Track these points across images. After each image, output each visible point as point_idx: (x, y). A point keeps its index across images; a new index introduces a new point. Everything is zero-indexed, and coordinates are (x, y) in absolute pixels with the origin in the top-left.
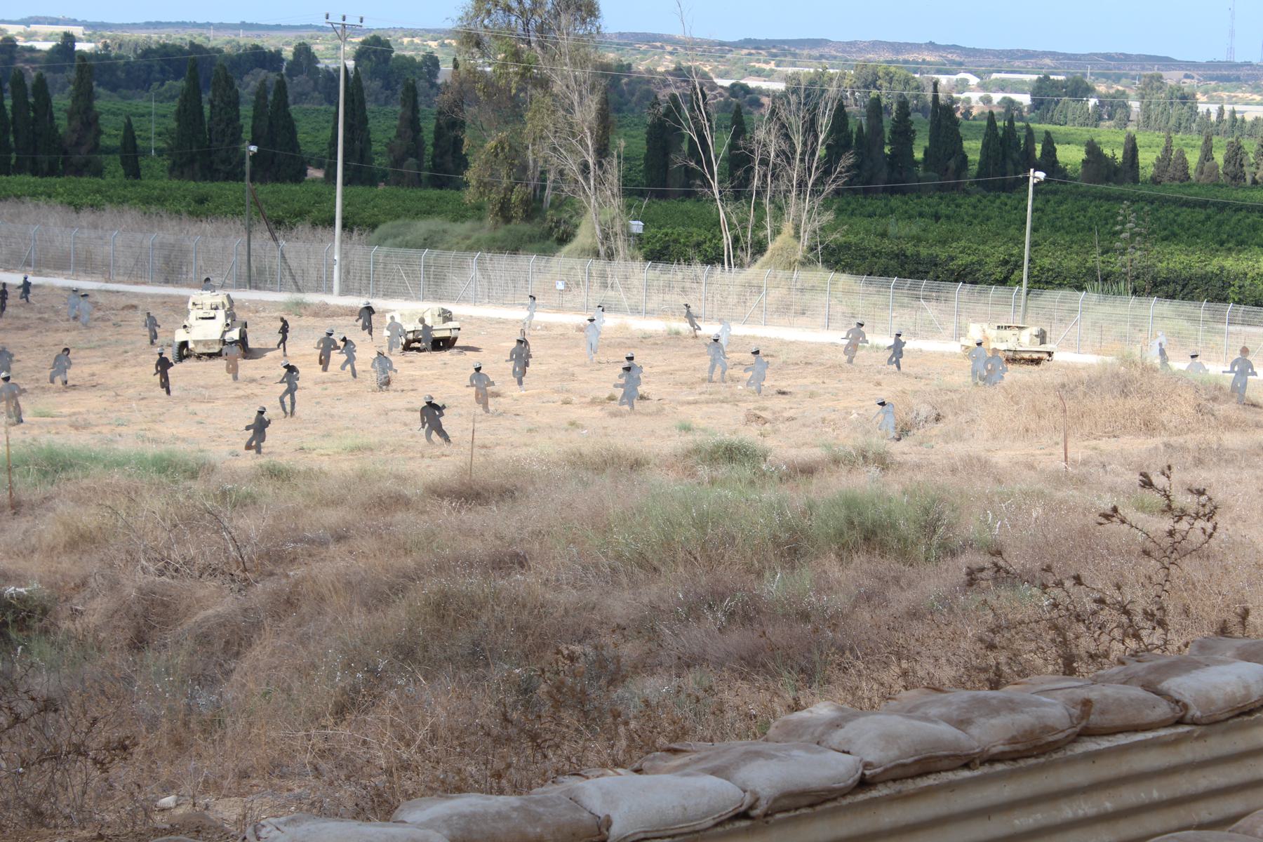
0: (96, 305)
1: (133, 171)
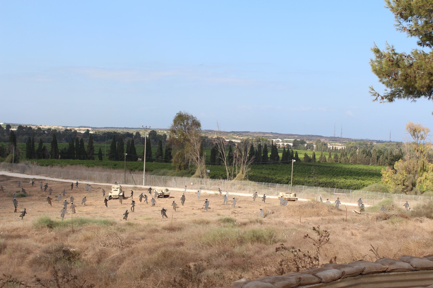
0: (92, 188)
1: (101, 159)
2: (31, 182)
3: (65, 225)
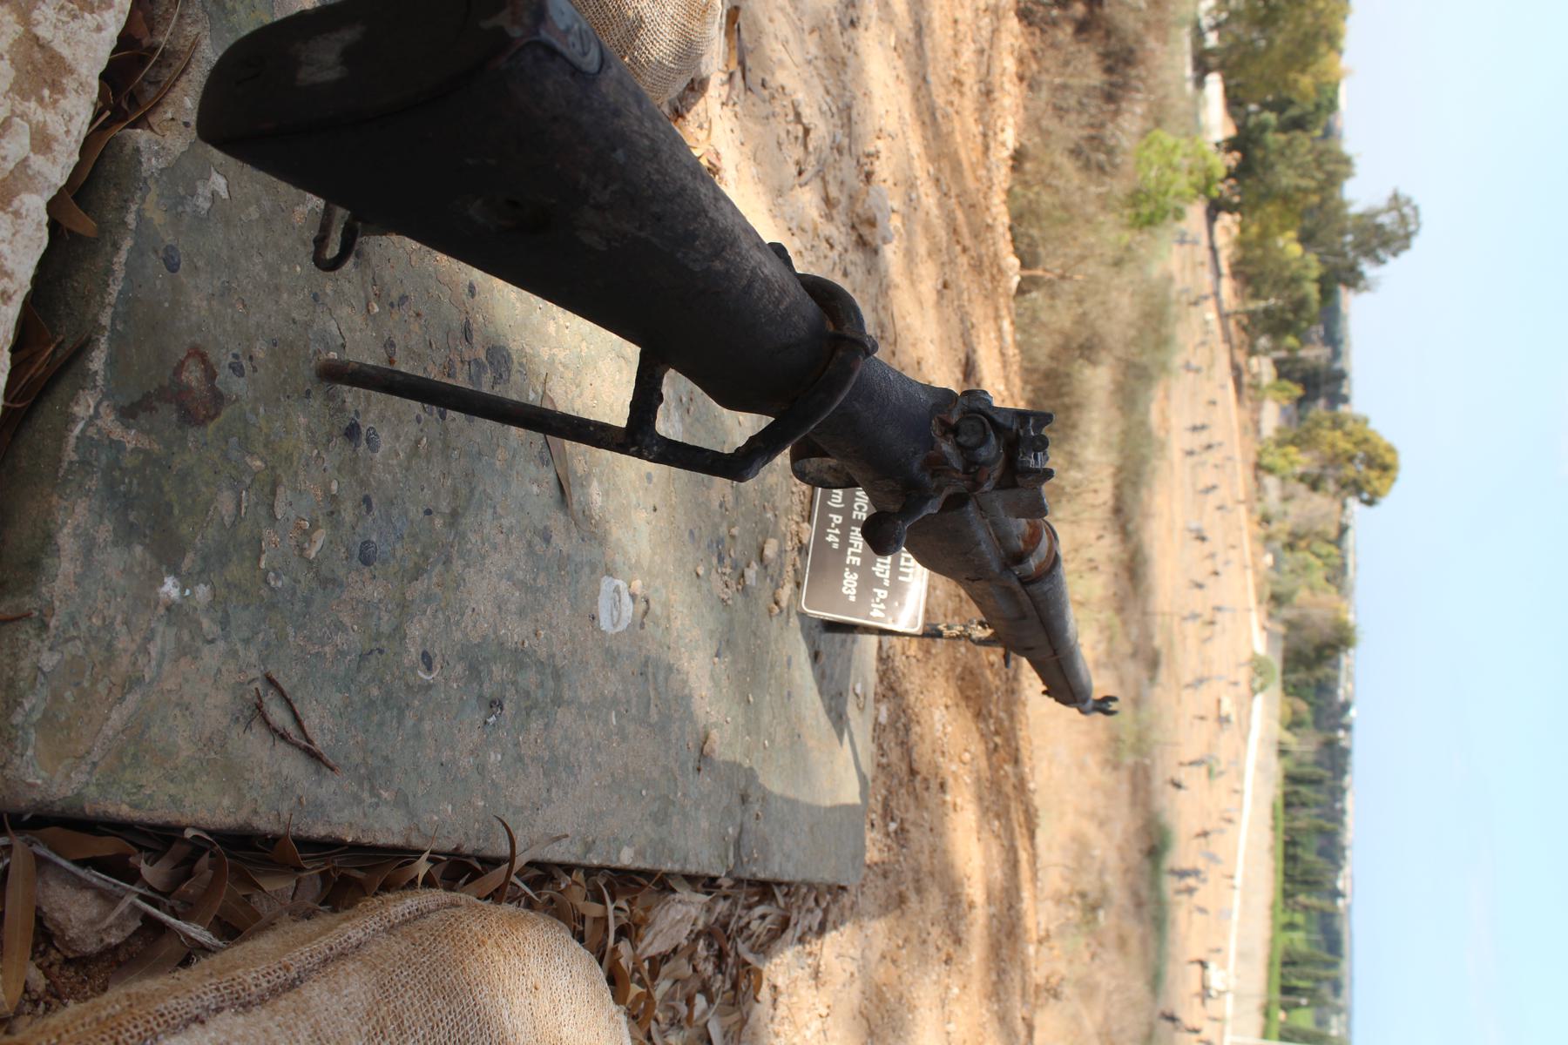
2: (1237, 787)
3: (1155, 885)
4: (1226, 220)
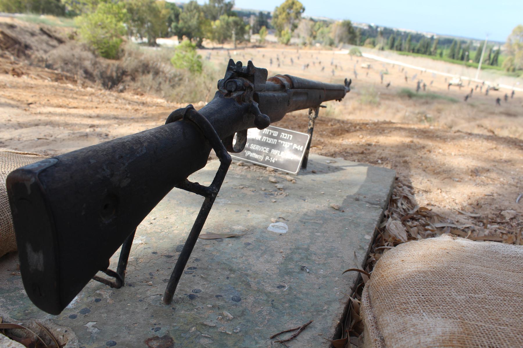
3: (421, 97)
4: (204, 43)
